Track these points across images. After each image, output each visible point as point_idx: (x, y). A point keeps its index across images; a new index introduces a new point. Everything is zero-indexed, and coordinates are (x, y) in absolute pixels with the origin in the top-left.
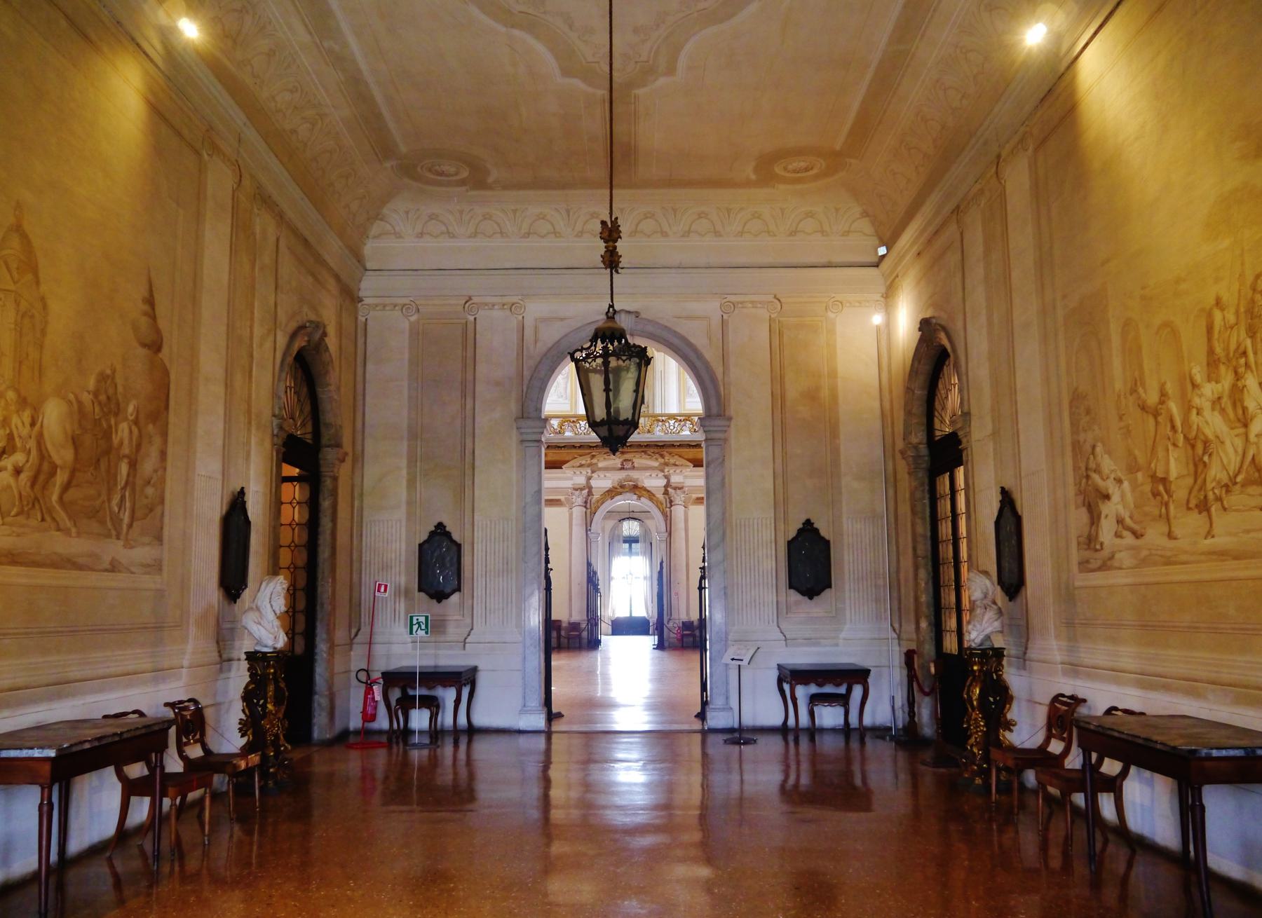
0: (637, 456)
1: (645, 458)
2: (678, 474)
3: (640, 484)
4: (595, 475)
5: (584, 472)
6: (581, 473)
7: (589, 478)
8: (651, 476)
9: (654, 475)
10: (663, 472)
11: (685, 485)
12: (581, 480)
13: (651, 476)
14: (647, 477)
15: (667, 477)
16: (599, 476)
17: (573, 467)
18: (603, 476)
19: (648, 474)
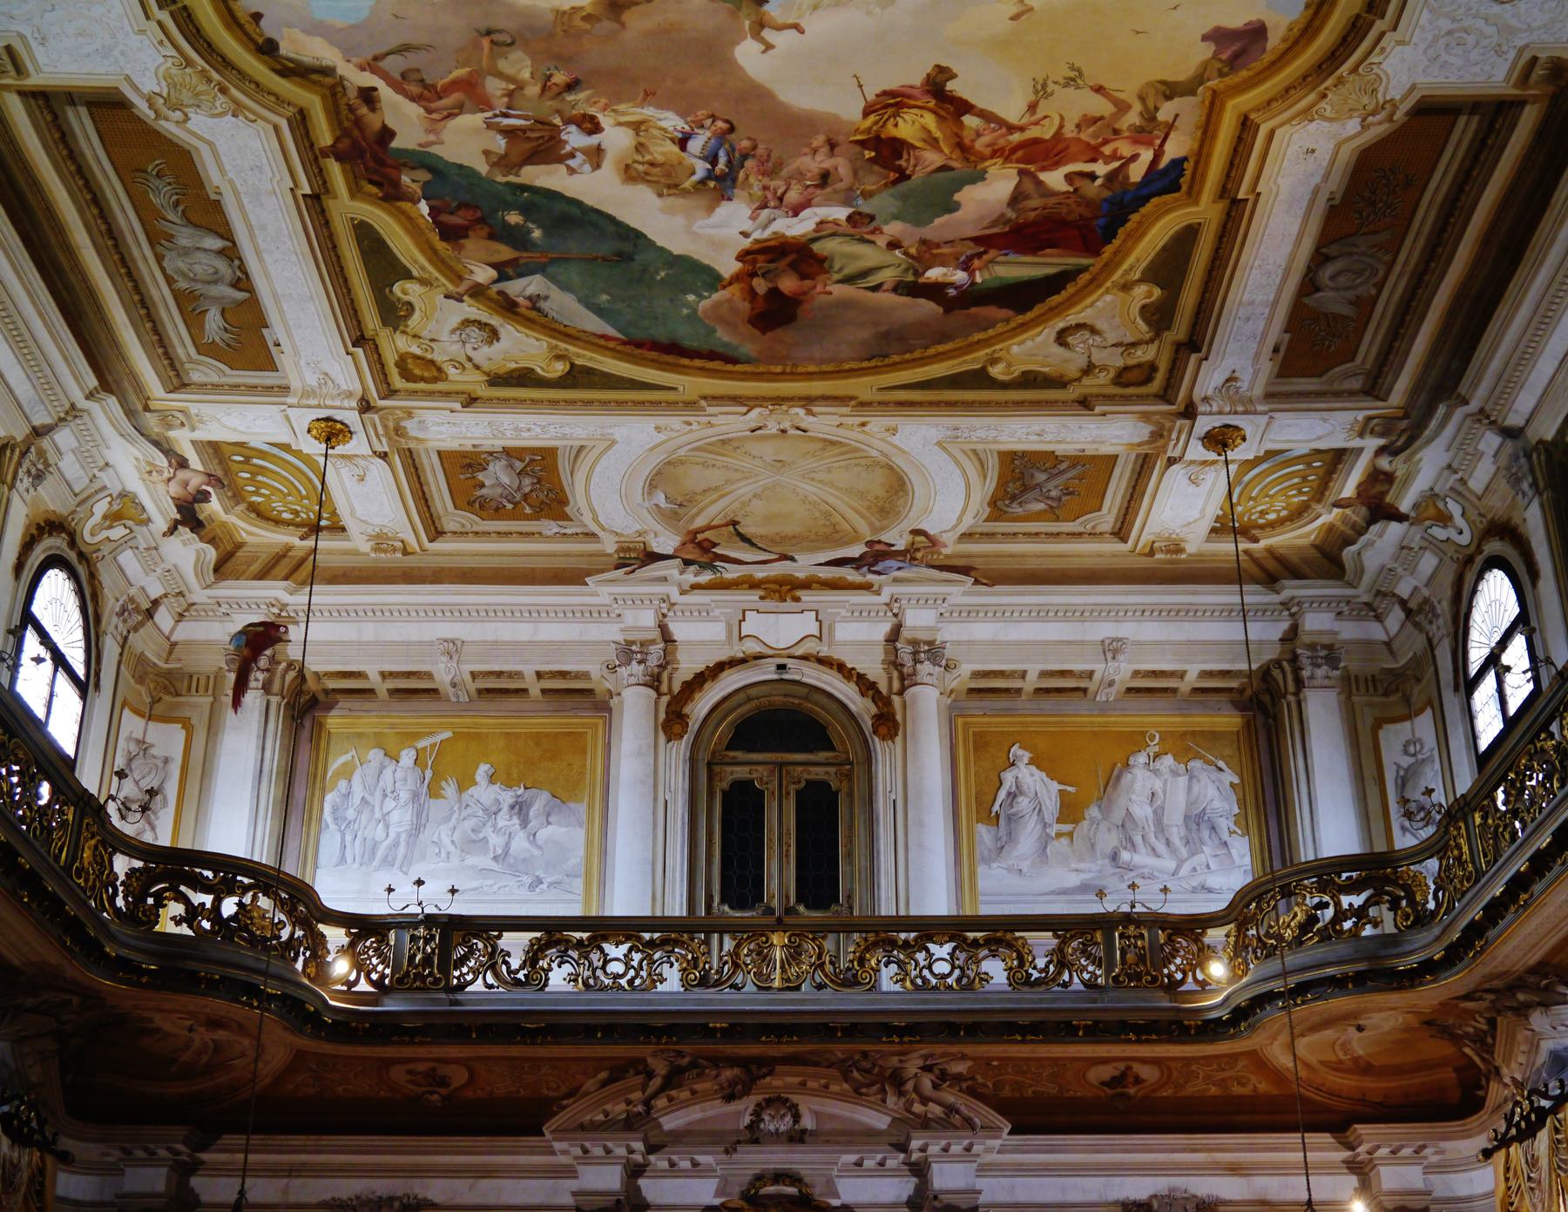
0: (811, 1084)
1: (841, 1097)
2: (956, 1159)
3: (818, 1192)
4: (659, 1162)
5: (621, 1151)
6: (608, 1151)
7: (635, 1171)
8: (859, 1164)
9: (869, 1163)
10: (903, 1148)
11: (982, 1199)
12: (606, 1179)
13: (859, 1164)
14: (846, 1171)
15: (919, 1170)
16: (672, 1164)
17: (582, 1127)
18: (685, 1164)
19: (853, 1158)
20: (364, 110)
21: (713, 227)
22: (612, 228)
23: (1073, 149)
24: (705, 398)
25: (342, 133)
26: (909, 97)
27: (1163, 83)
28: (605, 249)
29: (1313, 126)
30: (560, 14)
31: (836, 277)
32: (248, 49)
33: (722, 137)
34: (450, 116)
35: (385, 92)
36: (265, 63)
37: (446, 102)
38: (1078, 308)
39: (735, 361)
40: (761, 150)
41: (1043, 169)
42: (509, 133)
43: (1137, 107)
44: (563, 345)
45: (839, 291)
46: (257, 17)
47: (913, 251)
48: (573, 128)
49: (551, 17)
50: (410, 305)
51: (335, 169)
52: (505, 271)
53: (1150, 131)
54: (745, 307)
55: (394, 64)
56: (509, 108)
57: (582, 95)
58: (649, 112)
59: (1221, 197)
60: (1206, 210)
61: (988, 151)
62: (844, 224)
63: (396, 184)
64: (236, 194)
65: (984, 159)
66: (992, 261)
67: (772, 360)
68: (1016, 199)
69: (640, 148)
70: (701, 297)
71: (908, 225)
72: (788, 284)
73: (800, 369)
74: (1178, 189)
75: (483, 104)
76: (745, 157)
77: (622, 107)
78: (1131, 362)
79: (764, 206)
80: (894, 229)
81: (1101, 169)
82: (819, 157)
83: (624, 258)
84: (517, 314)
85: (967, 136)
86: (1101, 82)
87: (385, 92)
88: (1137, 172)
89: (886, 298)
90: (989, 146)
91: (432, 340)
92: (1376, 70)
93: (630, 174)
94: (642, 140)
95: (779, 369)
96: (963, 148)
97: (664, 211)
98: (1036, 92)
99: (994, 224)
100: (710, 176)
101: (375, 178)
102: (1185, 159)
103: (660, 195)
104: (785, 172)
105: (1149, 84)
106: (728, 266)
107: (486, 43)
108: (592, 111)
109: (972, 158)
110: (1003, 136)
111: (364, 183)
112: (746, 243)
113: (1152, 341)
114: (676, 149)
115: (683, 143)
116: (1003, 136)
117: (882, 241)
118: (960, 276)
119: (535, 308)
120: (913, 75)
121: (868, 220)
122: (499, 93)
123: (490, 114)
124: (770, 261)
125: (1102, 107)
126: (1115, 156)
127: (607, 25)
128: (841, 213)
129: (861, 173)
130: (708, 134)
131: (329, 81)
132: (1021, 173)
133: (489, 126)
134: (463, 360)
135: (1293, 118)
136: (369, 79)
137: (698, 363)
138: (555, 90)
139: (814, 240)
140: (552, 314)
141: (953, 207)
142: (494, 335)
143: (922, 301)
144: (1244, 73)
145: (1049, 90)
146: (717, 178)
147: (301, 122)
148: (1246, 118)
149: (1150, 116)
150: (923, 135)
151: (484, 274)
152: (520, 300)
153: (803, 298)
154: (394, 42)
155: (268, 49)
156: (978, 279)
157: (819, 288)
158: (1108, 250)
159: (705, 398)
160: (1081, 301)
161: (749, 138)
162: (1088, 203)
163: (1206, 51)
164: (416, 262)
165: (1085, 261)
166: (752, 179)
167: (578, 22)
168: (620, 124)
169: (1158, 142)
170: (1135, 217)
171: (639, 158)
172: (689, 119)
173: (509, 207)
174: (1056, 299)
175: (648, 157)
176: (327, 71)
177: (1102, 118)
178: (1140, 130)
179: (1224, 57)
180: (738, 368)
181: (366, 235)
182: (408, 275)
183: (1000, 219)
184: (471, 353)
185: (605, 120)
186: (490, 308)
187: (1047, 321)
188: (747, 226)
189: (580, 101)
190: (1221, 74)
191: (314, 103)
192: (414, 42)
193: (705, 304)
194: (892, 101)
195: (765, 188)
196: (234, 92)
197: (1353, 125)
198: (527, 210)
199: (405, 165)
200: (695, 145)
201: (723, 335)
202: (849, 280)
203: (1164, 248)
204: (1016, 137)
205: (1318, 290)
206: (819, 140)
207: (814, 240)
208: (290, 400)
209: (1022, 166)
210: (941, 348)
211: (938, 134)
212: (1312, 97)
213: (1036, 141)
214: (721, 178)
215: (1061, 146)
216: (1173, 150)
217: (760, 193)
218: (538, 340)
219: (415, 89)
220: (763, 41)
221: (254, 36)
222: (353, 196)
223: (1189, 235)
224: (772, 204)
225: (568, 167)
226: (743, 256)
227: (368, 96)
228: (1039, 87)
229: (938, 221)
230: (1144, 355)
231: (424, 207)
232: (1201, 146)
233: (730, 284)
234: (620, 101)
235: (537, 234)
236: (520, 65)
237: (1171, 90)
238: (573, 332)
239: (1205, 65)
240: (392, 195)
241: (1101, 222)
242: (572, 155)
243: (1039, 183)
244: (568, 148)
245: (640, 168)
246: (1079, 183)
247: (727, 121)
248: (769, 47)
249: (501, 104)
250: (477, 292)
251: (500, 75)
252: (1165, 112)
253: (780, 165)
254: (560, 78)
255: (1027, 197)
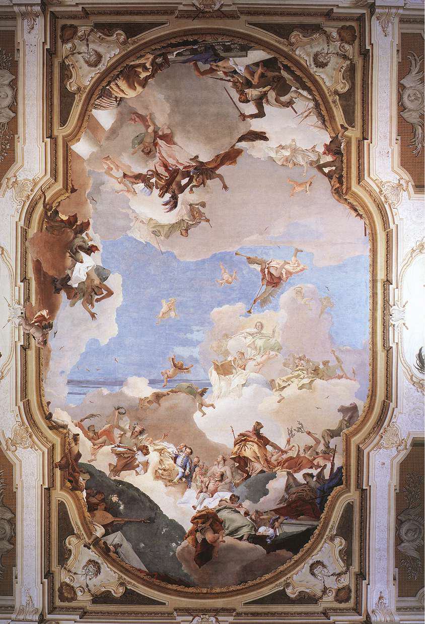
20: (73, 444)
21: (184, 503)
22: (148, 504)
23: (304, 462)
24: (175, 610)
25: (64, 456)
26: (249, 436)
27: (329, 430)
28: (145, 515)
29: (381, 451)
30: (141, 400)
31: (227, 532)
32: (43, 417)
33: (188, 457)
34: (101, 446)
35: (82, 437)
36: (46, 423)
37: (100, 440)
38: (315, 552)
39: (188, 585)
40: (200, 463)
41: (295, 472)
42: (119, 455)
43: (322, 441)
44: (124, 576)
45: (229, 540)
46: (49, 403)
47: (253, 517)
48: (140, 452)
49: (138, 402)
50: (70, 550)
51: (58, 472)
52: (110, 529)
53: (329, 453)
54: (193, 549)
55: (86, 423)
56: (120, 443)
57: (144, 436)
58: (165, 444)
59: (358, 488)
60: (353, 496)
61: (275, 463)
62: (228, 501)
63: (77, 481)
64: (23, 487)
65: (275, 467)
66: (282, 523)
67: (205, 585)
68: (288, 487)
69: (161, 462)
70: (178, 545)
71: (251, 502)
72: (209, 536)
73: (214, 591)
74: (342, 484)
75: (111, 441)
76: (196, 466)
77: (156, 442)
78: (341, 586)
79: (201, 492)
80: (247, 504)
81: (315, 472)
82: (220, 466)
83: (151, 520)
84: (109, 556)
85: (269, 456)
86: (309, 430)
87: (82, 437)
88: (327, 474)
89: (245, 544)
90: (276, 460)
91: (75, 573)
92: (395, 425)
93: (157, 477)
94: (162, 458)
95: (205, 591)
96: (267, 461)
97: (168, 494)
98: (289, 434)
99: (281, 501)
100: (184, 476)
101: (71, 478)
102: (342, 467)
103: (166, 486)
104: (208, 474)
105: (325, 431)
106: (188, 527)
107: (117, 414)
108: (147, 444)
109: (271, 467)
110: (280, 455)
111: (67, 481)
112: (194, 513)
113: (345, 573)
114: (172, 462)
115: (175, 459)
116: (280, 455)
117: (242, 513)
118: (270, 532)
119: (116, 553)
120: (249, 427)
121: (237, 499)
122: (118, 436)
123: (113, 446)
124: (203, 523)
125: (311, 442)
126: (318, 466)
127: (155, 405)
128: (227, 495)
129: (234, 473)
130: (184, 455)
131: (65, 431)
132: (288, 473)
133: (113, 451)
134: (84, 586)
135: (374, 447)
136: (77, 430)
137: (174, 587)
138: (136, 434)
139: (219, 511)
140: (122, 556)
141: (266, 492)
142: (98, 571)
143: (258, 546)
144: (354, 426)
145: (293, 433)
146: (186, 477)
147: (52, 449)
148: (359, 447)
149: (327, 445)
150: (254, 455)
151: (99, 531)
152: (111, 547)
153: (214, 545)
154: (88, 414)
155: (48, 417)
156: (278, 534)
157: (220, 539)
158: (323, 516)
159: (175, 610)
160: (316, 547)
161: (197, 457)
162: (312, 490)
163: (340, 416)
164: (77, 525)
165: (315, 523)
166: (197, 477)
167: (146, 404)
168: (155, 450)
169: (332, 458)
170: (329, 498)
171: (160, 467)
172: (178, 448)
173: (113, 492)
174: (307, 546)
175: (163, 466)
176: (65, 427)
177: (312, 447)
178: (325, 453)
179: (346, 419)
180: (191, 590)
181: (62, 506)
182: (74, 534)
183: (283, 500)
184: (89, 582)
185: (151, 449)
186: (99, 552)
187: (305, 559)
188: (195, 502)
189: (144, 440)
190: (347, 427)
191: (57, 440)
192: (95, 413)
193: (179, 548)
194: (243, 439)
195: (202, 482)
196: (34, 437)
197: (394, 451)
198: (120, 494)
199: (81, 471)
200: (179, 460)
201: (185, 569)
202: (231, 534)
203: (342, 516)
204: (285, 456)
205: (402, 542)
206: (220, 458)
207: (219, 511)
208: (13, 616)
209: (288, 470)
210: (267, 576)
211: (259, 455)
212: (378, 437)
213: (291, 458)
214: (186, 477)
215: (300, 461)
216: (339, 462)
217: (200, 484)
218: (115, 572)
219: (91, 434)
220: (202, 411)
221: (45, 410)
222: (61, 489)
223: (349, 508)
224: (204, 490)
225: (136, 472)
226: (194, 520)
227: (76, 437)
228: (290, 432)
229: (262, 500)
230: (345, 581)
231: (84, 494)
232: (346, 461)
233: (188, 536)
234: (156, 439)
235: (122, 507)
236: (126, 423)
237: (333, 434)
238: (127, 567)
239: (341, 422)
240: (75, 487)
241: (318, 501)
242: (138, 466)
243: (295, 479)
244: (137, 462)
245: (160, 472)
246: (309, 479)
247: (190, 449)
248: (204, 414)
249: (117, 440)
250: (96, 542)
251: (119, 427)
252: (333, 442)
253: (206, 471)
254: (138, 429)
255: (291, 487)
